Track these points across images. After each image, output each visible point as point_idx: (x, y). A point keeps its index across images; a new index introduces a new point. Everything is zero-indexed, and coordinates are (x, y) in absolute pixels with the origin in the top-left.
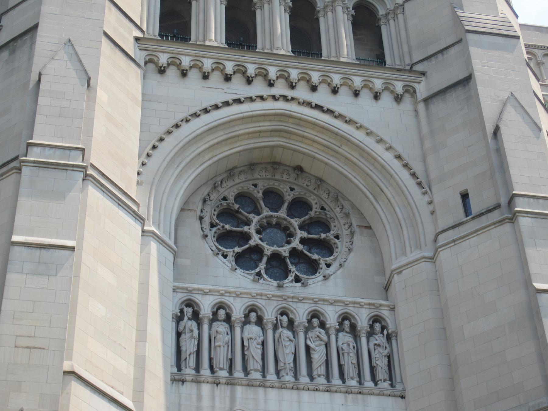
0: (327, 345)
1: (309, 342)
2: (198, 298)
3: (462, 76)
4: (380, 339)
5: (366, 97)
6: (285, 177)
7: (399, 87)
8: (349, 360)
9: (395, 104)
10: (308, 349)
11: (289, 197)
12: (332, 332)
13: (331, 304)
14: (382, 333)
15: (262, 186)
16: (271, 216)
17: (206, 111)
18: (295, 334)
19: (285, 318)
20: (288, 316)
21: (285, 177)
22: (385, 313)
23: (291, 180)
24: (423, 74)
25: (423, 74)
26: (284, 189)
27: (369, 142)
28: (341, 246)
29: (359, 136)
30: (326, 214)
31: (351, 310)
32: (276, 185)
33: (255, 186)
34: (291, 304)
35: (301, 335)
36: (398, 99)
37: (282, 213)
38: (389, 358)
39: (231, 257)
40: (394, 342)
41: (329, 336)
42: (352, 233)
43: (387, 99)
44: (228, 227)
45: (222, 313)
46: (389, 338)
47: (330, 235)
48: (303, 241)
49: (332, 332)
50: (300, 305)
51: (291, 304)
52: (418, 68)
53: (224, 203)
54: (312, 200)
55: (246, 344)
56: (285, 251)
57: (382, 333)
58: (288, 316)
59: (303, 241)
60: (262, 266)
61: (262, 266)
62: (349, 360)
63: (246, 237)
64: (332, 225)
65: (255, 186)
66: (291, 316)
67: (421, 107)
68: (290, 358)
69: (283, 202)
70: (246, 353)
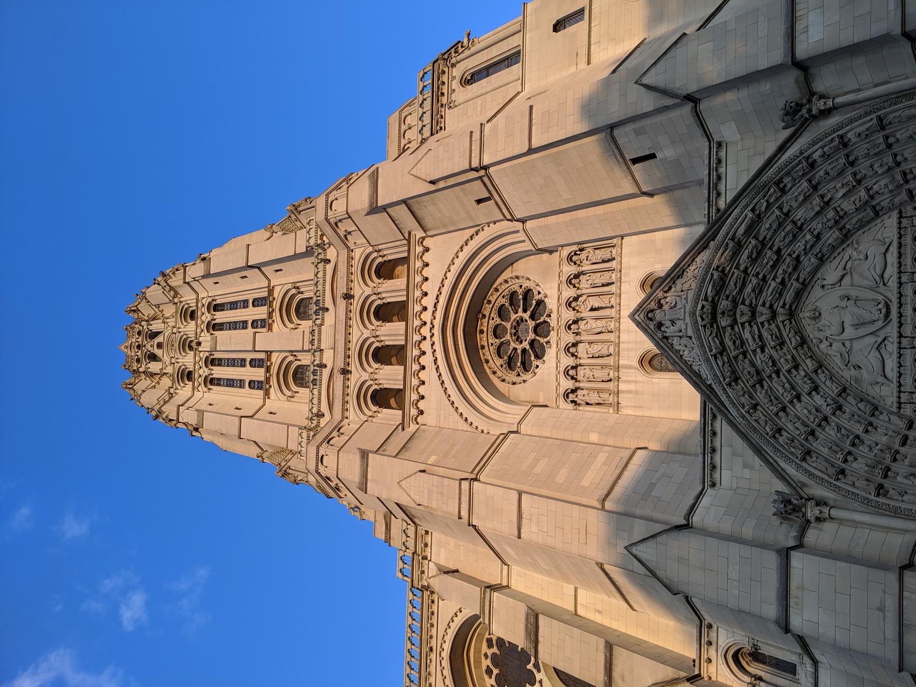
10: (592, 309)
11: (498, 321)
13: (561, 293)
18: (582, 319)
19: (572, 327)
20: (570, 325)
28: (526, 284)
31: (564, 279)
34: (562, 323)
37: (508, 325)
39: (538, 362)
44: (519, 364)
47: (520, 291)
48: (525, 311)
49: (579, 292)
56: (531, 324)
59: (525, 311)
60: (542, 340)
61: (542, 340)
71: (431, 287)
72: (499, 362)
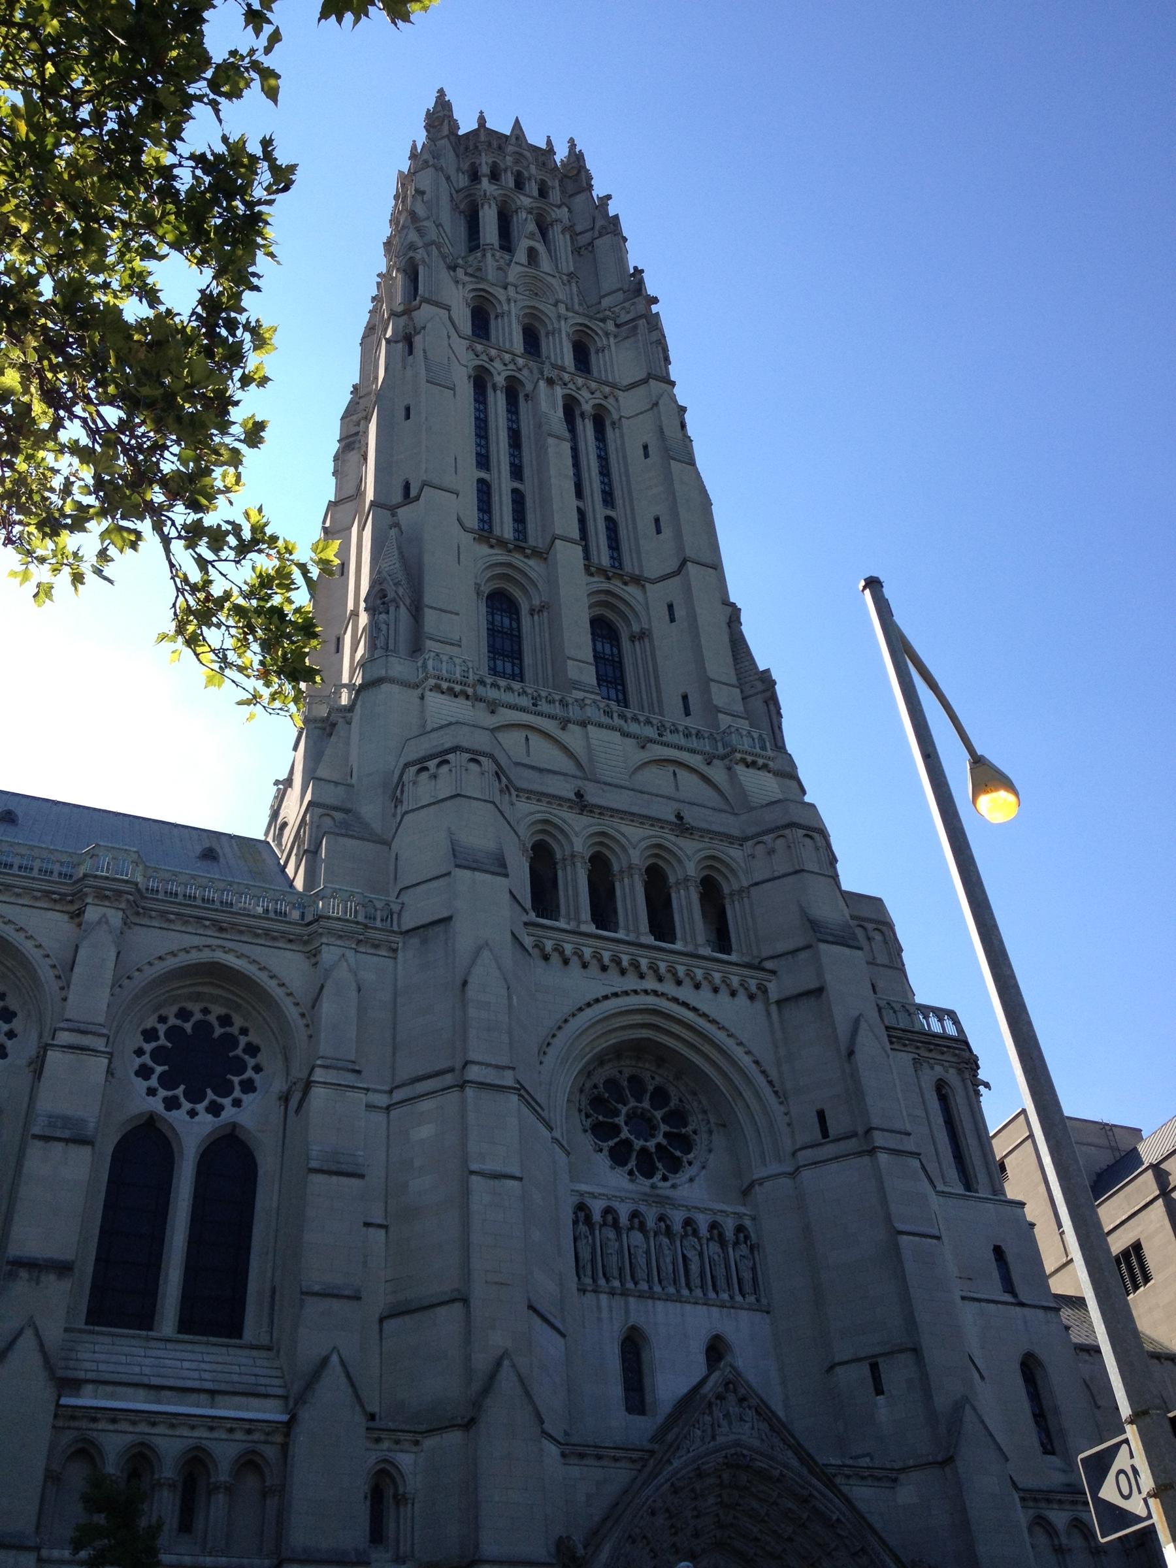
0: (701, 1254)
1: (685, 1252)
2: (589, 1201)
3: (813, 985)
4: (744, 1249)
5: (724, 996)
6: (647, 1066)
7: (753, 985)
8: (720, 1272)
9: (748, 1002)
10: (684, 1256)
12: (704, 1241)
13: (702, 1212)
14: (745, 1243)
15: (627, 1072)
16: (637, 1107)
18: (672, 1242)
19: (662, 1224)
20: (665, 1222)
21: (647, 1066)
22: (747, 1222)
23: (653, 1069)
24: (774, 972)
25: (774, 972)
26: (646, 1076)
27: (729, 1043)
28: (701, 1140)
29: (720, 1036)
30: (684, 1107)
31: (719, 1219)
33: (620, 1072)
34: (668, 1211)
35: (678, 1243)
36: (752, 997)
38: (754, 1269)
39: (606, 1152)
40: (756, 1253)
41: (701, 1245)
42: (710, 1132)
43: (742, 998)
44: (601, 1118)
45: (610, 1218)
46: (752, 1248)
47: (689, 1129)
48: (666, 1135)
49: (704, 1241)
50: (676, 1212)
51: (668, 1211)
52: (769, 965)
53: (595, 1091)
54: (672, 1091)
55: (632, 1251)
56: (651, 1145)
57: (745, 1243)
58: (665, 1222)
59: (666, 1135)
60: (632, 1163)
61: (632, 1163)
62: (720, 1272)
63: (616, 1129)
64: (690, 1119)
65: (620, 1072)
66: (668, 1222)
67: (774, 1009)
68: (670, 1268)
69: (645, 1091)
70: (633, 1261)
71: (703, 1000)
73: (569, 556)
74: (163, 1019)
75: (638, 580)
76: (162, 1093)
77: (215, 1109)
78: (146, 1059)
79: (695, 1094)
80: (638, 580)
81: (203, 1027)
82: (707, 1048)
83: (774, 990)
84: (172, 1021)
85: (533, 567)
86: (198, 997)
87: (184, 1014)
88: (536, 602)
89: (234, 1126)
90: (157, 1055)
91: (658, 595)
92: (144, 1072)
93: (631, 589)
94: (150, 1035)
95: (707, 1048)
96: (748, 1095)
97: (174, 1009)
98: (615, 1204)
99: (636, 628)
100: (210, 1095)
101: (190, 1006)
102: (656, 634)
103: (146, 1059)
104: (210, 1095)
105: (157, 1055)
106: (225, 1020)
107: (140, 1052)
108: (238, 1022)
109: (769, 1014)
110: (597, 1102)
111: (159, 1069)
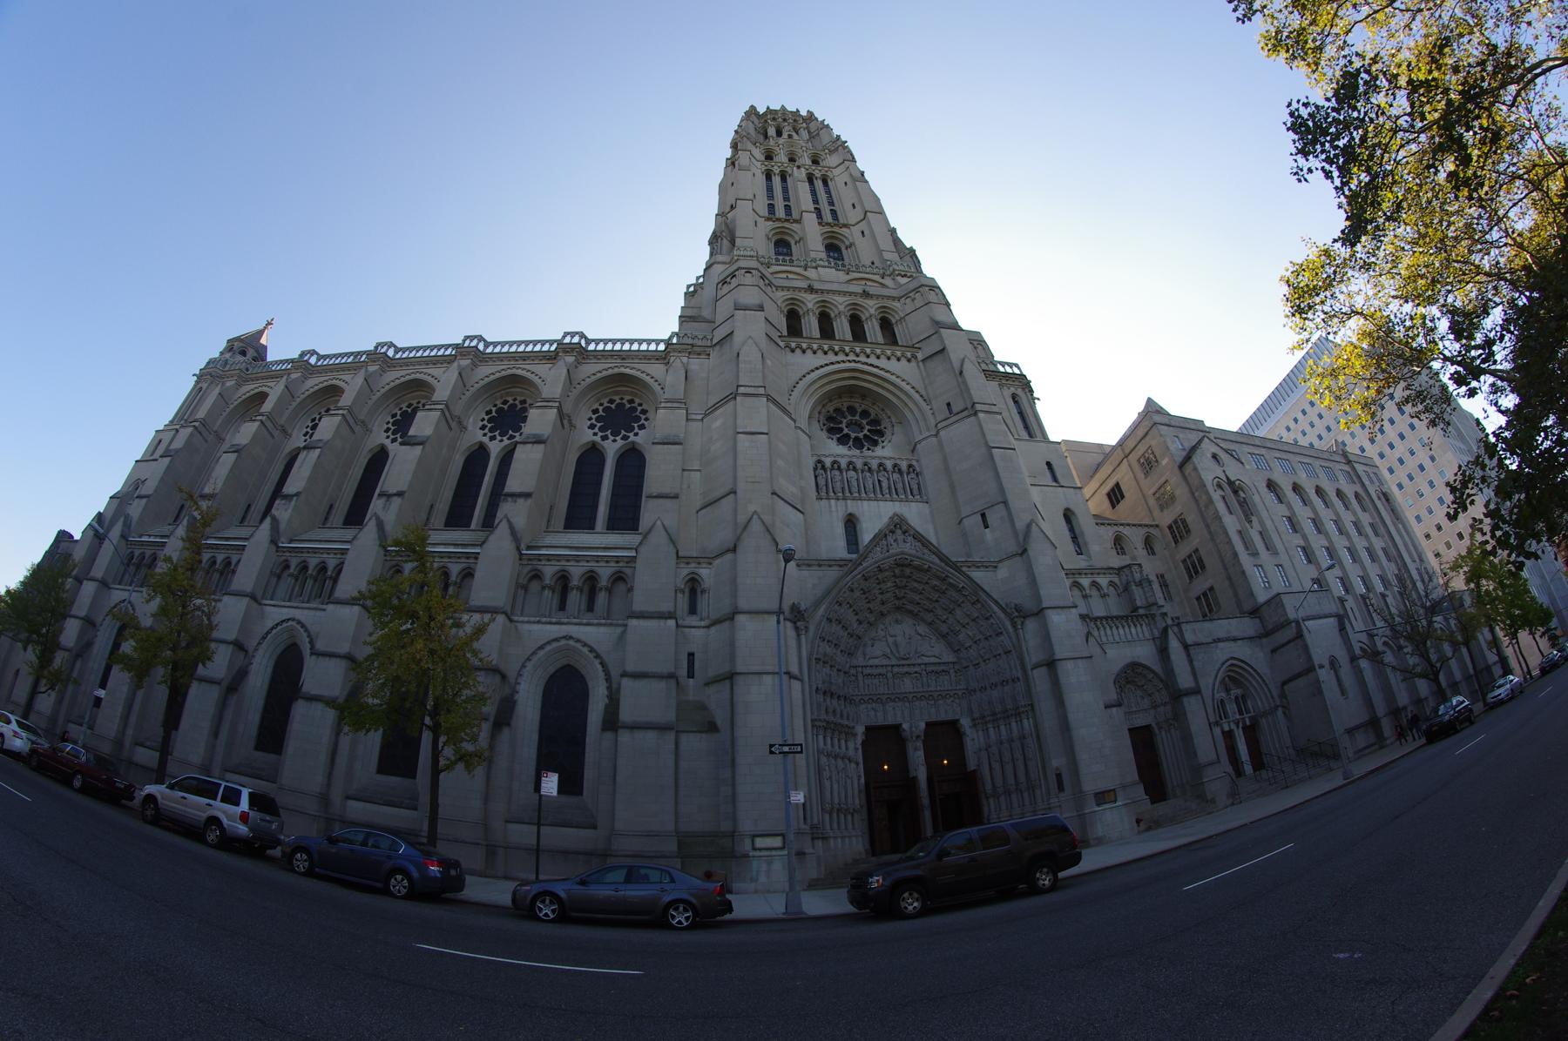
0: (888, 479)
2: (823, 459)
4: (913, 475)
5: (894, 360)
7: (909, 355)
8: (900, 486)
11: (859, 410)
17: (817, 369)
18: (872, 474)
22: (914, 463)
26: (857, 405)
27: (898, 381)
28: (888, 432)
29: (893, 378)
31: (898, 462)
32: (851, 404)
36: (909, 361)
37: (857, 418)
38: (919, 484)
43: (904, 361)
45: (836, 466)
48: (869, 431)
54: (871, 411)
56: (861, 435)
59: (869, 431)
60: (851, 443)
61: (851, 443)
62: (900, 486)
63: (842, 430)
67: (921, 364)
72: (831, 409)
73: (810, 220)
74: (601, 405)
75: (845, 226)
76: (600, 434)
77: (625, 438)
78: (593, 421)
79: (883, 410)
80: (845, 226)
81: (620, 406)
82: (886, 385)
83: (920, 356)
84: (606, 405)
85: (795, 226)
86: (617, 393)
87: (611, 401)
88: (798, 239)
89: (633, 443)
90: (598, 419)
91: (856, 230)
92: (592, 427)
93: (844, 229)
94: (595, 411)
95: (886, 385)
96: (911, 405)
97: (607, 400)
98: (839, 459)
99: (847, 243)
100: (623, 432)
101: (614, 398)
102: (857, 243)
103: (593, 421)
104: (623, 432)
105: (598, 419)
106: (631, 401)
107: (590, 419)
108: (637, 401)
109: (918, 366)
110: (830, 419)
111: (599, 425)
